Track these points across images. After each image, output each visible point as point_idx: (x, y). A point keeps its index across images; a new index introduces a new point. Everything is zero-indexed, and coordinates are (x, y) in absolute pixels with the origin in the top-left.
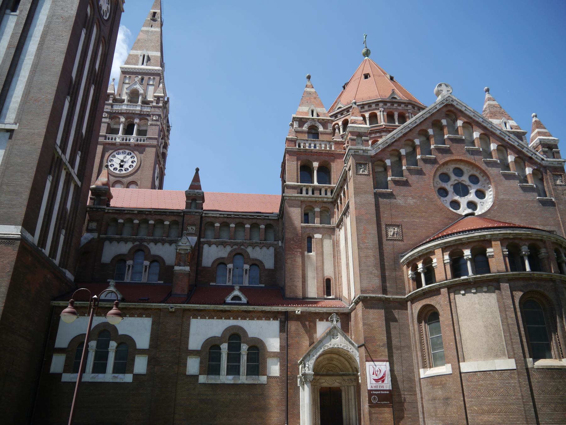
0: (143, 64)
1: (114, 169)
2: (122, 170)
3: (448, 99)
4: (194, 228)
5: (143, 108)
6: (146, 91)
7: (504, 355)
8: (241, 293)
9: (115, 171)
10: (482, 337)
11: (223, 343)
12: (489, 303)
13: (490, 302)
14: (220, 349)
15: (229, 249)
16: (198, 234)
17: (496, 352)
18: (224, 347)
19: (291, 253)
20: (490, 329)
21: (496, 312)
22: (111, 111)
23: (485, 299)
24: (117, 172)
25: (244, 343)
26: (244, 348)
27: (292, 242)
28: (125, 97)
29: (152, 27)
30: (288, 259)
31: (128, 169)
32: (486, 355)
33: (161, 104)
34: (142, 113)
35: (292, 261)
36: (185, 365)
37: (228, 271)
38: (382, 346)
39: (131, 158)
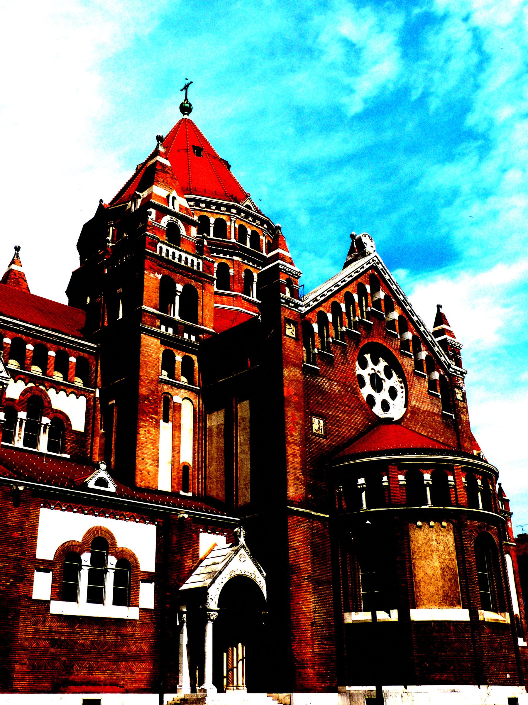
7: (459, 604)
8: (109, 476)
10: (437, 580)
11: (85, 551)
12: (447, 541)
13: (448, 540)
14: (80, 561)
17: (451, 599)
18: (86, 558)
19: (144, 418)
20: (447, 572)
21: (453, 553)
23: (444, 536)
25: (112, 554)
26: (112, 561)
27: (146, 402)
30: (141, 427)
32: (441, 603)
35: (145, 431)
36: (31, 583)
37: (18, 423)
38: (306, 579)
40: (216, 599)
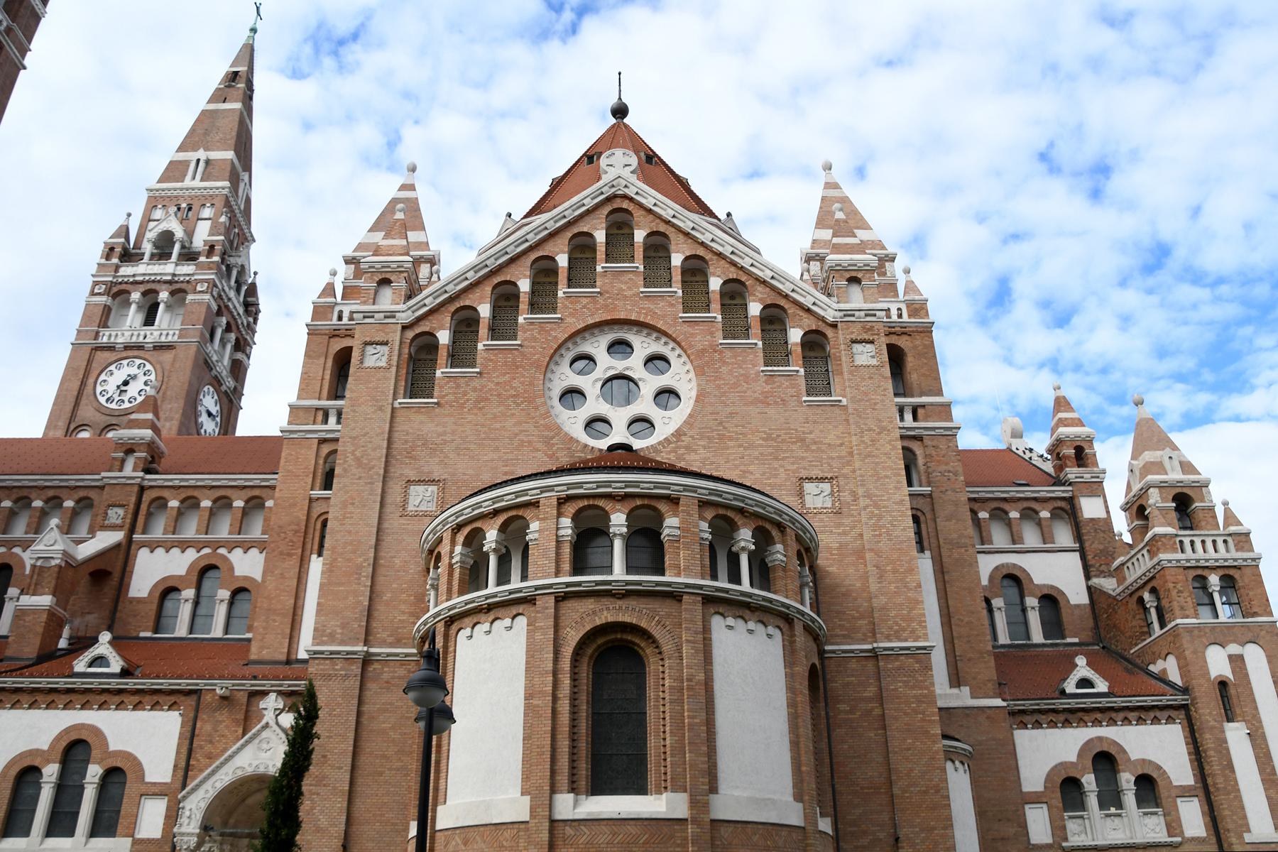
0: (194, 178)
1: (108, 400)
2: (123, 401)
3: (614, 183)
4: (121, 512)
5: (179, 268)
6: (190, 233)
9: (109, 405)
15: (191, 555)
16: (127, 526)
22: (115, 280)
24: (113, 406)
26: (94, 772)
28: (147, 248)
29: (224, 102)
31: (135, 399)
33: (216, 259)
34: (176, 279)
39: (145, 374)
40: (198, 817)
